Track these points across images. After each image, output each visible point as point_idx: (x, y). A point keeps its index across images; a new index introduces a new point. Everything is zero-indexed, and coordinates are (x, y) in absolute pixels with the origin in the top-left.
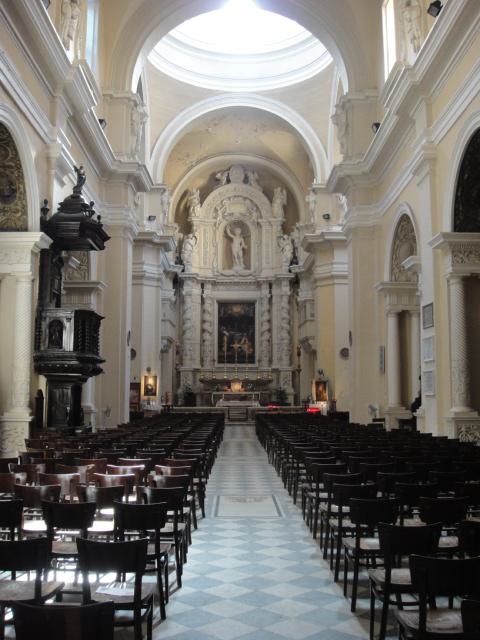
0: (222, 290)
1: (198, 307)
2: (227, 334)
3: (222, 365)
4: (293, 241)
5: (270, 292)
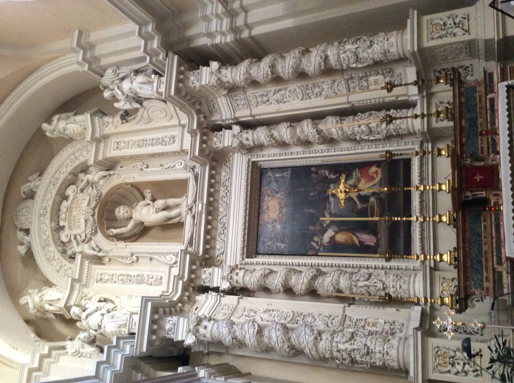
0: (225, 242)
1: (247, 302)
2: (329, 233)
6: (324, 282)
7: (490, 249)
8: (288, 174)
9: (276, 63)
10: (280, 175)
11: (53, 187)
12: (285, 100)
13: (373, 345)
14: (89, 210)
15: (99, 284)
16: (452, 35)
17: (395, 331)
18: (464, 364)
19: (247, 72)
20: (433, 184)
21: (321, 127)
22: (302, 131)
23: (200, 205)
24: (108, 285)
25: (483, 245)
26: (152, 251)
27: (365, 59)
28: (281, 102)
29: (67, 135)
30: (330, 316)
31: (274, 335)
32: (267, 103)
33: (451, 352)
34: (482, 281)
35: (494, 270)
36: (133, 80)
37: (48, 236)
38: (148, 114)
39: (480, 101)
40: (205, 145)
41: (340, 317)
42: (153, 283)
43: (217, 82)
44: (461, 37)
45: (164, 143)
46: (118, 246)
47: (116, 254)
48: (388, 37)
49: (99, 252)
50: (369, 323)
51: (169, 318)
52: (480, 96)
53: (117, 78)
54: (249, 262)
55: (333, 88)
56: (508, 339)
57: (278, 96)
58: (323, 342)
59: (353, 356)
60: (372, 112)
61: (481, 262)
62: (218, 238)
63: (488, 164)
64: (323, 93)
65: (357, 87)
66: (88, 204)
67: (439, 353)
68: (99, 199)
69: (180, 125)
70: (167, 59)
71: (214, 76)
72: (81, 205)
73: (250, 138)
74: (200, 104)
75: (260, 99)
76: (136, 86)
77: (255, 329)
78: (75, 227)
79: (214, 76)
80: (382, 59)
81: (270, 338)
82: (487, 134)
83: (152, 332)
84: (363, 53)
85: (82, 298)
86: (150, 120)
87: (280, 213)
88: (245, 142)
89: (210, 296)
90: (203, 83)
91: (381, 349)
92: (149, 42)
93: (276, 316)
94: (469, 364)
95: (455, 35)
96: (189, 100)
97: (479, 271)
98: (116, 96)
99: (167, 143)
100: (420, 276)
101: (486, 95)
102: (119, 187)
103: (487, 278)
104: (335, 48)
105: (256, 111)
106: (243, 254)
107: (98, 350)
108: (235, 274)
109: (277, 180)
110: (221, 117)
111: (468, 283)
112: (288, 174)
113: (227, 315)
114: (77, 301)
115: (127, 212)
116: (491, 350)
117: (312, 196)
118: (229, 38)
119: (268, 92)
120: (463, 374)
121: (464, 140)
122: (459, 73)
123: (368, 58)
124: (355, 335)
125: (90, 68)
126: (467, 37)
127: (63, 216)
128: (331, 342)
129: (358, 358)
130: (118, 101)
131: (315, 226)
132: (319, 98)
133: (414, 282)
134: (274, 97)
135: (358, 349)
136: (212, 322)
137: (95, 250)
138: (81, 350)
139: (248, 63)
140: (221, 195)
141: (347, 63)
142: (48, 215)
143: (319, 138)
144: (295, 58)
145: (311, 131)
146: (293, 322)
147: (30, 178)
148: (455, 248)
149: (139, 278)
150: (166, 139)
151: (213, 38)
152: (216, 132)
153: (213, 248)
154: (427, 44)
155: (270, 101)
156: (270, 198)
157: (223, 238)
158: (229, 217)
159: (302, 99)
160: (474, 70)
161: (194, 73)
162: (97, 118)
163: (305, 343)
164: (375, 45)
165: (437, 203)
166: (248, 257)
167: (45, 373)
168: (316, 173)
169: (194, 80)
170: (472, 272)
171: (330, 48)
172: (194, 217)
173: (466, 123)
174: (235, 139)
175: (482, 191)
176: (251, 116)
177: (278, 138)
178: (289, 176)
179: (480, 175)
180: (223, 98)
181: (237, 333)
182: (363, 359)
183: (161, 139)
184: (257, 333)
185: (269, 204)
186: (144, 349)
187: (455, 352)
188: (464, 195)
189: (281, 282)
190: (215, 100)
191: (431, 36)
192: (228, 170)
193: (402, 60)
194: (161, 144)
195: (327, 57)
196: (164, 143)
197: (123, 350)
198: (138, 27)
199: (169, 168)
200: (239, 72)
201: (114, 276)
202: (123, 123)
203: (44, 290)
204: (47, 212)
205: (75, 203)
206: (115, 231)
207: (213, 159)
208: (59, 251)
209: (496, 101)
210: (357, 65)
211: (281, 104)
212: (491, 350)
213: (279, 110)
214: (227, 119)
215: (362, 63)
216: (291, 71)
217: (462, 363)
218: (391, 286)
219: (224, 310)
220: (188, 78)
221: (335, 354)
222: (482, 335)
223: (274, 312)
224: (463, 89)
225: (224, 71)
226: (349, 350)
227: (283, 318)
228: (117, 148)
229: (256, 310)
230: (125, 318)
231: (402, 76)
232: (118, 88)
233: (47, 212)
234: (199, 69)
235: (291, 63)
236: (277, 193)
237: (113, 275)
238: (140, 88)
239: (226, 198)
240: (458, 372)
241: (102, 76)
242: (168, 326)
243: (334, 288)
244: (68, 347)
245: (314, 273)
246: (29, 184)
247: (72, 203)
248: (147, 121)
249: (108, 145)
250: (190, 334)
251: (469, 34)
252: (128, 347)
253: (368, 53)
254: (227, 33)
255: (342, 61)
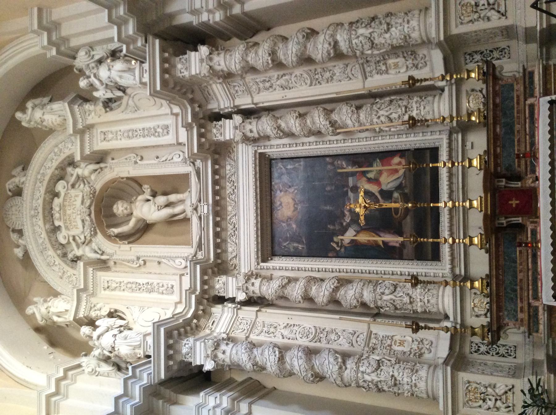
0: (237, 245)
2: (350, 235)
3: (445, 250)
4: (100, 62)
5: (229, 116)
6: (346, 295)
7: (526, 276)
8: (300, 165)
9: (277, 48)
10: (292, 167)
11: (41, 184)
12: (291, 85)
13: (400, 376)
14: (85, 210)
15: (107, 292)
16: (486, 20)
17: (422, 351)
18: (496, 400)
19: (244, 59)
20: (464, 201)
21: (335, 117)
22: (314, 123)
23: (206, 207)
24: (117, 293)
25: (518, 272)
26: (159, 255)
27: (382, 45)
28: (286, 88)
29: (46, 127)
30: (355, 333)
31: (296, 363)
32: (271, 90)
33: (482, 388)
34: (517, 312)
35: (529, 304)
36: (111, 67)
37: (44, 239)
38: (133, 102)
39: (518, 103)
40: (203, 140)
41: (365, 334)
42: (164, 292)
43: (209, 72)
44: (496, 22)
45: (157, 134)
46: (122, 249)
47: (120, 258)
48: (409, 18)
49: (102, 255)
50: (396, 341)
51: (185, 342)
52: (518, 97)
53: (92, 61)
54: (265, 267)
55: (346, 72)
56: (543, 378)
57: (282, 81)
58: (348, 371)
59: (380, 387)
60: (393, 98)
61: (515, 291)
62: (229, 241)
63: (526, 187)
64: (334, 77)
65: (374, 71)
66: (82, 203)
67: (470, 388)
68: (94, 197)
69: (172, 114)
70: (147, 45)
71: (204, 64)
72: (74, 203)
73: (255, 130)
74: (193, 92)
75: (261, 85)
76: (114, 74)
77: (275, 356)
78: (72, 227)
79: (204, 64)
80: (403, 44)
81: (292, 365)
82: (524, 156)
83: (168, 357)
84: (379, 38)
85: (91, 308)
86: (137, 108)
87: (294, 211)
88: (249, 134)
89: (226, 309)
90: (193, 73)
91: (409, 380)
92: (123, 28)
93: (297, 333)
94: (500, 400)
95: (489, 19)
96: (179, 90)
97: (513, 300)
98: (94, 84)
99: (161, 134)
100: (449, 289)
101: (525, 100)
102: (113, 181)
103: (522, 309)
104: (345, 32)
105: (257, 99)
106: (258, 258)
107: (115, 368)
108: (251, 284)
109: (289, 173)
110: (219, 105)
111: (501, 314)
112: (300, 165)
113: (245, 331)
114: (86, 312)
115: (126, 209)
116: (525, 394)
117: (329, 191)
118: (218, 16)
119: (270, 78)
120: (495, 409)
121: (498, 150)
122: (494, 65)
123: (385, 44)
124: (381, 365)
125: (58, 52)
126: (504, 22)
127: (57, 215)
128: (357, 371)
129: (385, 388)
130: (97, 90)
131: (334, 225)
132: (330, 84)
133: (443, 296)
134: (278, 83)
135: (385, 381)
136: (231, 345)
137: (98, 253)
138: (98, 369)
139: (244, 49)
140: (228, 192)
141: (361, 49)
142: (41, 216)
143: (333, 130)
144: (298, 43)
145: (323, 123)
146: (315, 340)
147: (14, 173)
148: (487, 275)
149: (149, 286)
150: (158, 130)
151: (199, 15)
152: (215, 122)
153: (225, 251)
154: (455, 30)
155: (274, 86)
156: (282, 193)
157: (234, 240)
158: (239, 217)
159: (311, 85)
160: (511, 52)
161: (180, 59)
162: (76, 106)
163: (329, 373)
164: (394, 29)
165: (468, 220)
166: (263, 261)
167: (64, 396)
168: (332, 164)
169: (182, 69)
170: (505, 302)
171: (339, 31)
172: (200, 218)
173: (501, 130)
174: (238, 131)
175: (518, 217)
176: (253, 104)
177: (286, 129)
178: (302, 168)
179: (516, 200)
180: (218, 85)
181: (258, 359)
182: (391, 390)
183: (153, 130)
184: (279, 361)
185: (282, 200)
186: (163, 376)
187: (486, 387)
188: (497, 222)
189: (300, 294)
190: (209, 87)
191: (460, 21)
192: (233, 163)
193: (426, 43)
194: (154, 135)
195: (336, 43)
196: (157, 134)
197: (141, 379)
198: (107, 10)
199: (166, 160)
200: (233, 60)
201: (122, 284)
202: (106, 112)
203: (49, 302)
204: (38, 213)
205: (68, 201)
206: (116, 231)
207: (216, 152)
208: (58, 255)
209: (536, 108)
210: (372, 52)
211: (286, 90)
212: (525, 394)
213: (285, 98)
214: (226, 108)
215: (379, 50)
216: (294, 59)
217: (493, 399)
218: (419, 300)
219: (242, 325)
220: (174, 66)
221: (361, 384)
222: (515, 357)
223: (296, 328)
224: (497, 88)
225: (216, 58)
226: (375, 381)
227: (305, 335)
228: (104, 139)
229: (276, 325)
230: (139, 339)
231: (427, 59)
232: (95, 76)
233: (38, 213)
234: (186, 54)
235: (294, 50)
236: (290, 187)
237: (121, 282)
238: (121, 77)
239: (234, 196)
240: (489, 408)
241: (74, 58)
242: (184, 350)
243: (358, 301)
244: (83, 364)
245: (335, 285)
246: (13, 180)
247: (64, 200)
248: (134, 110)
249: (93, 136)
250: (209, 359)
251: (506, 18)
252: (145, 375)
253: (384, 38)
254: (215, 11)
255: (355, 47)
